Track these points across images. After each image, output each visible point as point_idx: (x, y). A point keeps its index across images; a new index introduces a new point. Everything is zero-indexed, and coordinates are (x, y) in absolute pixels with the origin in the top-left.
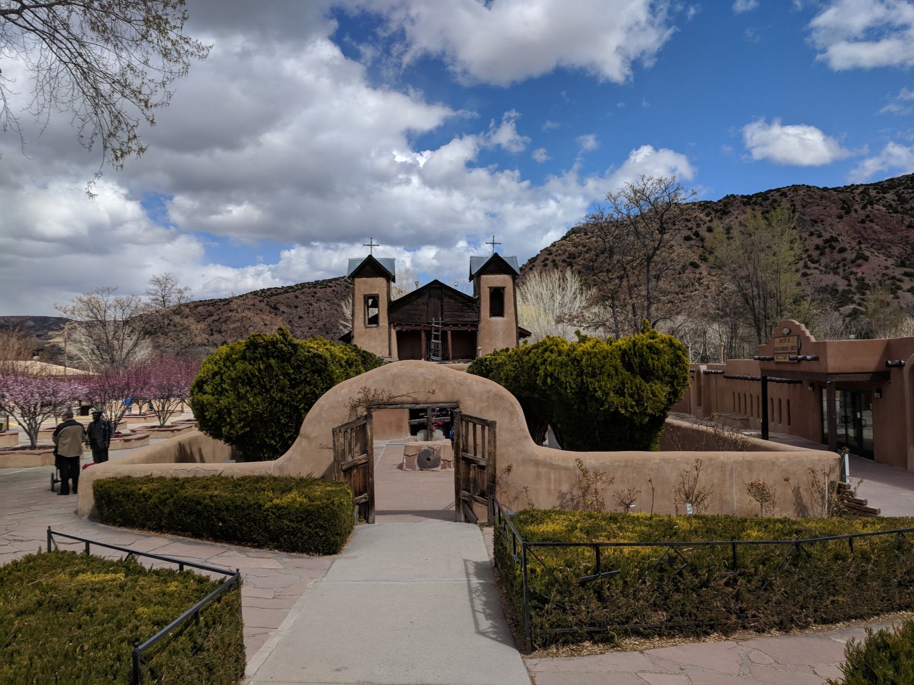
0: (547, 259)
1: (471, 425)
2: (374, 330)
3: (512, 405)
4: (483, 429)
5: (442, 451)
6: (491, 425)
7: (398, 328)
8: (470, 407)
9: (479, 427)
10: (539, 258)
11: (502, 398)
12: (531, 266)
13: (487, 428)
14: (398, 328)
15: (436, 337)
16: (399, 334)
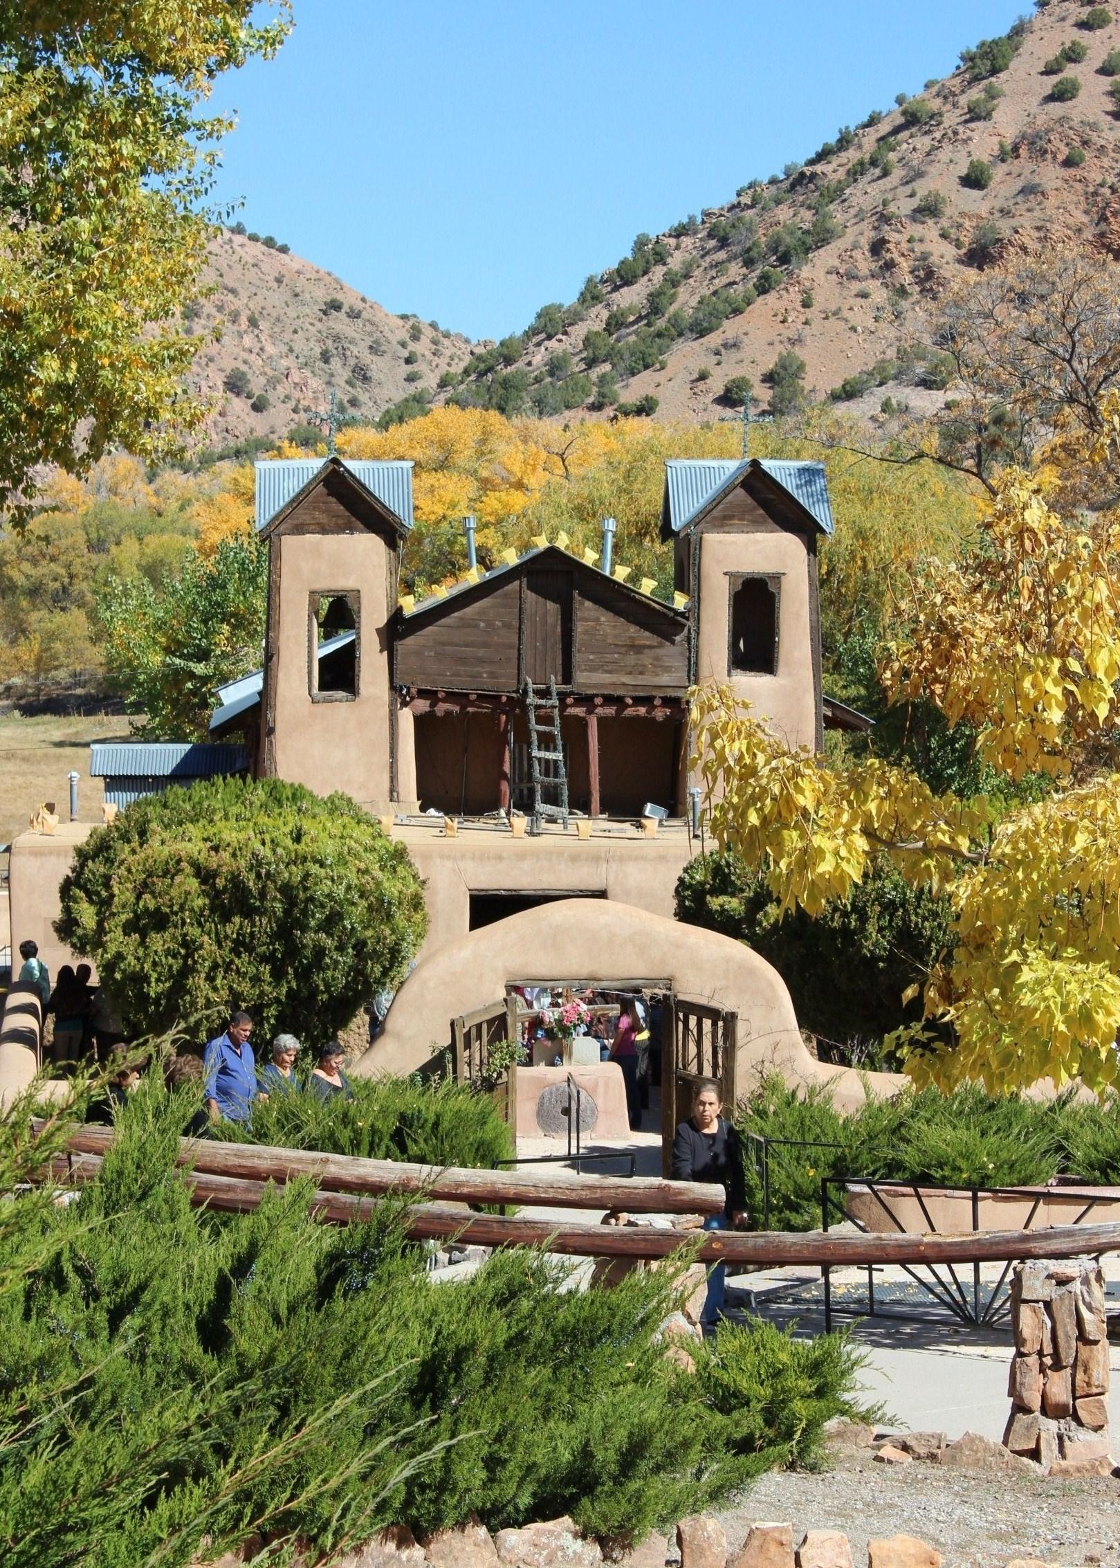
0: (1073, 55)
1: (693, 1021)
2: (340, 708)
3: (771, 985)
4: (715, 1024)
5: (601, 1090)
6: (731, 1018)
7: (422, 705)
8: (692, 990)
9: (707, 1024)
10: (1029, 43)
11: (752, 972)
12: (976, 93)
13: (720, 1024)
14: (422, 705)
15: (547, 742)
16: (421, 722)
